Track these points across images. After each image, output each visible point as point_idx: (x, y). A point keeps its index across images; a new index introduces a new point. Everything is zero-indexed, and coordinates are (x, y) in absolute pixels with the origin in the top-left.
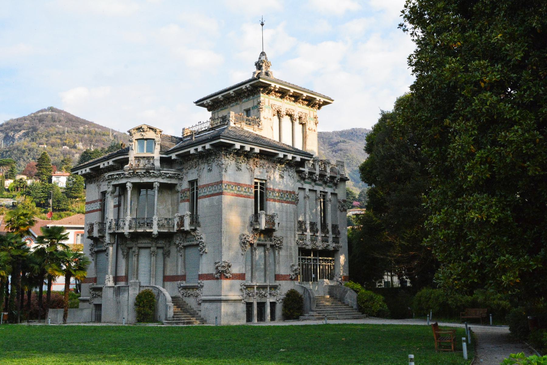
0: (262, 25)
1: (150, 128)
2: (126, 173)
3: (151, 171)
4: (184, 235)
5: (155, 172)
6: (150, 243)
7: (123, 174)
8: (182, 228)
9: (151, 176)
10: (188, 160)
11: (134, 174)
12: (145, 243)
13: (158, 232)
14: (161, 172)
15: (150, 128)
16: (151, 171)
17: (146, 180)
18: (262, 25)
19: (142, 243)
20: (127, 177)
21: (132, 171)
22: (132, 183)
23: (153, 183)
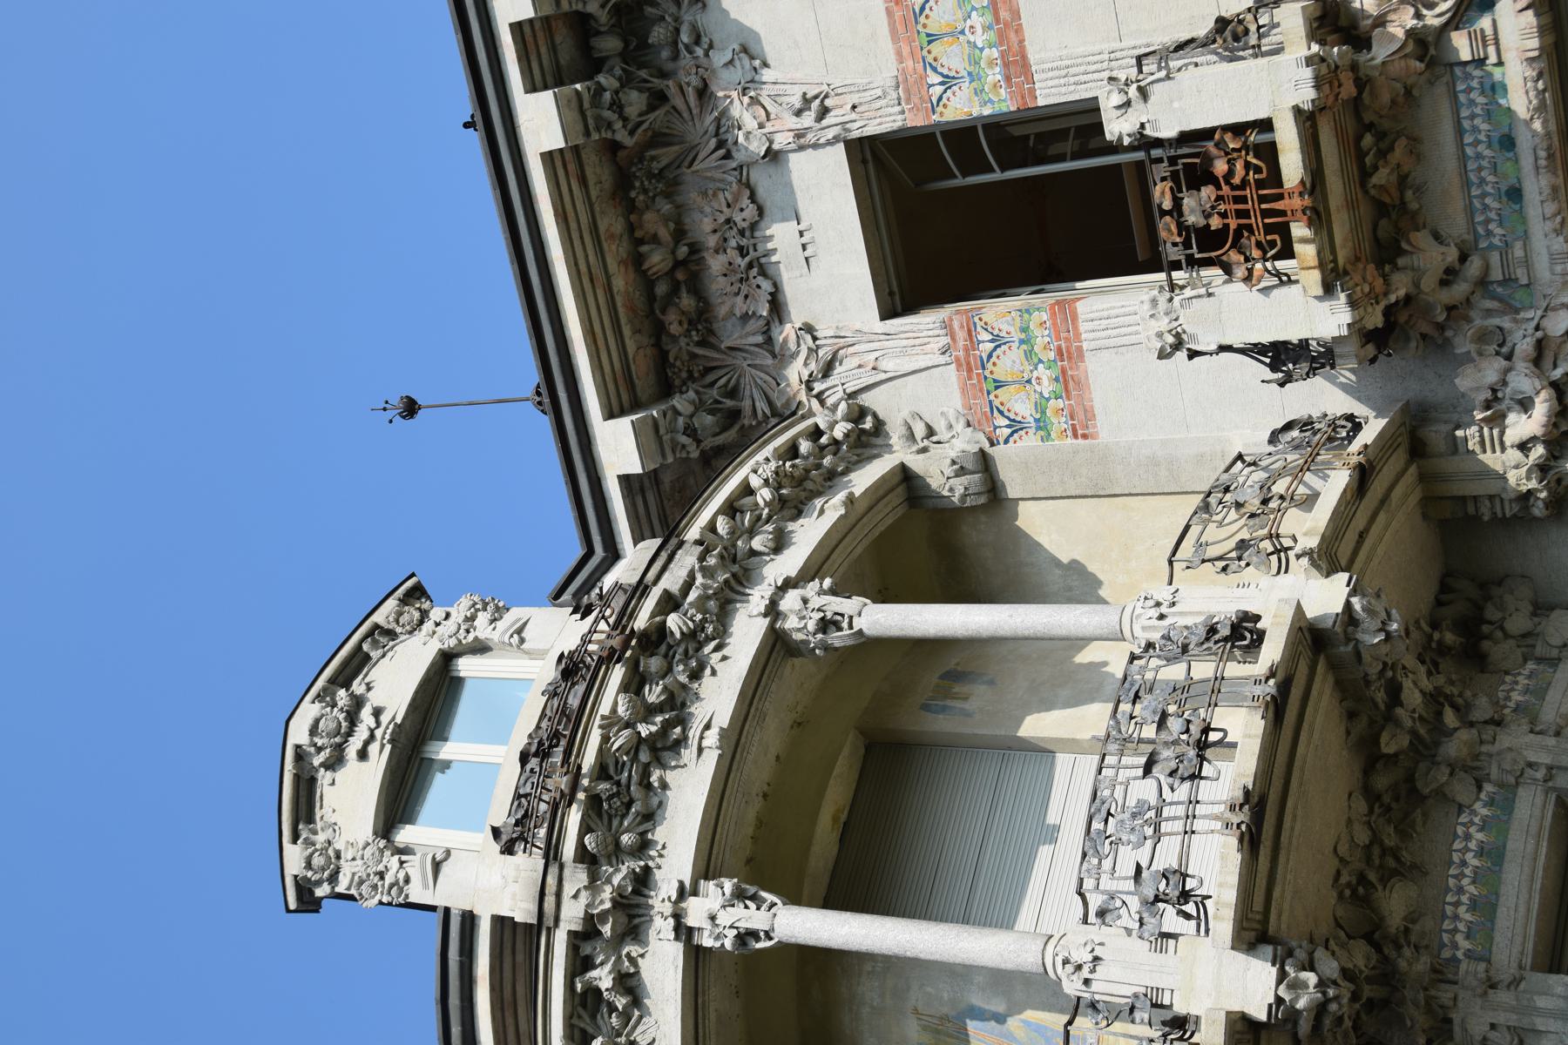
0: (410, 408)
1: (344, 678)
2: (572, 914)
3: (641, 622)
4: (1431, 257)
5: (672, 581)
6: (1505, 803)
7: (580, 964)
8: (1292, 166)
9: (694, 637)
10: (703, 320)
11: (622, 805)
12: (1494, 855)
13: (1327, 559)
14: (693, 533)
15: (344, 678)
16: (641, 622)
17: (718, 698)
18: (410, 408)
19: (1486, 907)
20: (631, 913)
21: (574, 818)
22: (707, 867)
23: (777, 645)
